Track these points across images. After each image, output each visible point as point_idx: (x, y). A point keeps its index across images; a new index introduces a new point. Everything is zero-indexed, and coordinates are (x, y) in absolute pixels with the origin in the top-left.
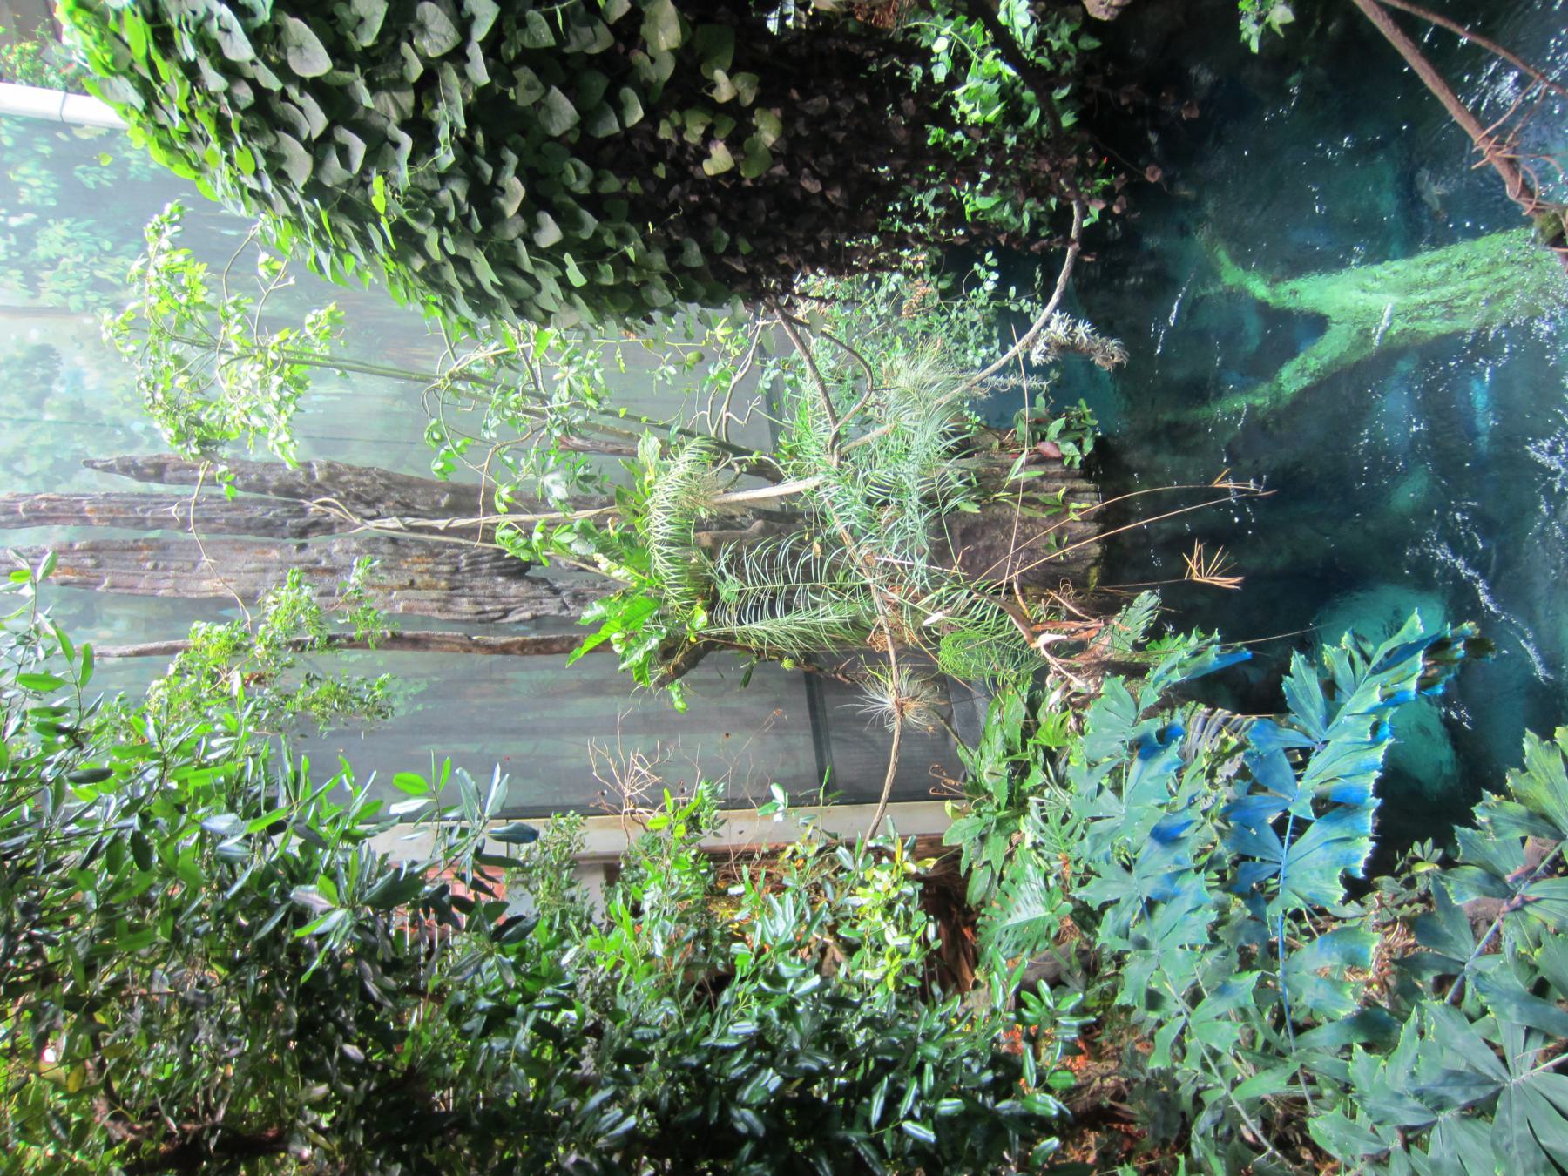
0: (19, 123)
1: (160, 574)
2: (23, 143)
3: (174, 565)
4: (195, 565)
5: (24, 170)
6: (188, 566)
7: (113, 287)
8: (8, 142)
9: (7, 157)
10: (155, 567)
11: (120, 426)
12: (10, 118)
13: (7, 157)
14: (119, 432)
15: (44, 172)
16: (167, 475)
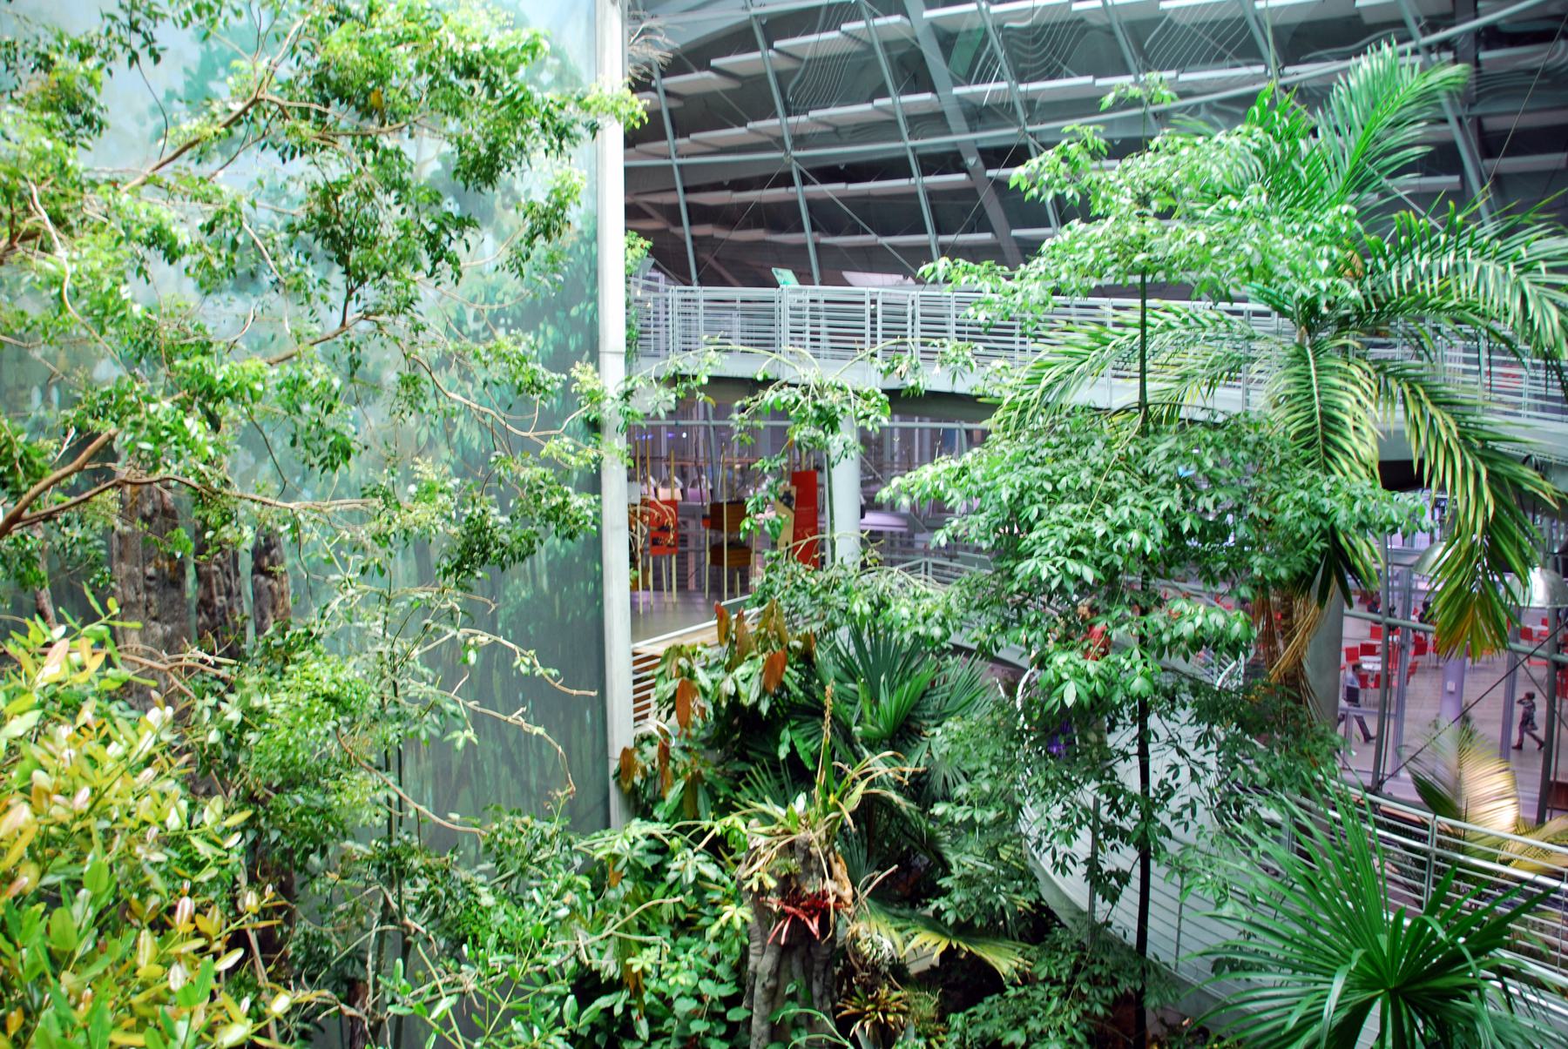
0: (592, 318)
1: (140, 584)
2: (576, 324)
3: (153, 597)
4: (155, 619)
5: (550, 331)
6: (153, 611)
7: (449, 436)
8: (574, 312)
9: (560, 314)
10: (151, 578)
11: (304, 479)
12: (596, 309)
13: (560, 314)
14: (298, 479)
15: (551, 348)
16: (262, 578)
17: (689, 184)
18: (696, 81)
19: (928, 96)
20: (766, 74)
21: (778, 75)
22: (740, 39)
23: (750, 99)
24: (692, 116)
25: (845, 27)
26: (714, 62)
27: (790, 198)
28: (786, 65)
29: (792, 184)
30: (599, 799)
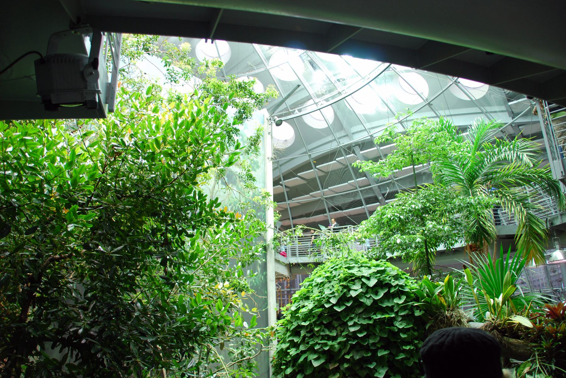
12: (265, 215)
17: (294, 216)
18: (294, 181)
19: (365, 178)
20: (315, 179)
21: (319, 177)
22: (307, 166)
23: (310, 186)
24: (294, 192)
25: (337, 159)
26: (298, 174)
27: (326, 219)
28: (321, 174)
29: (326, 213)
30: (266, 370)
